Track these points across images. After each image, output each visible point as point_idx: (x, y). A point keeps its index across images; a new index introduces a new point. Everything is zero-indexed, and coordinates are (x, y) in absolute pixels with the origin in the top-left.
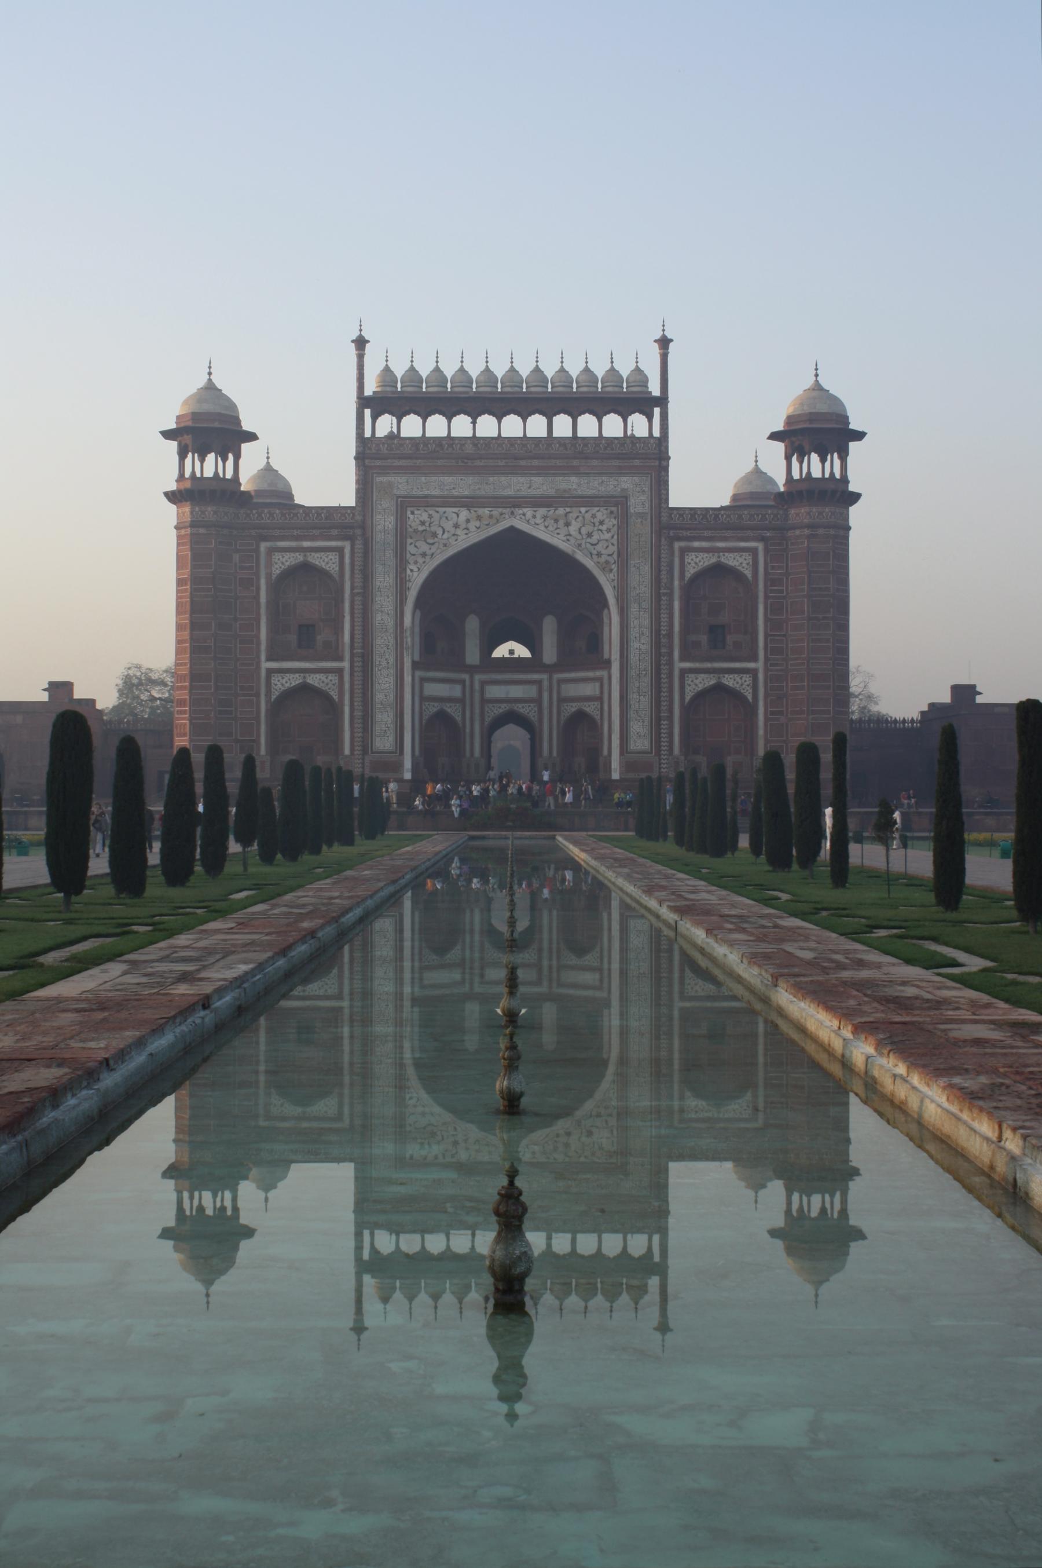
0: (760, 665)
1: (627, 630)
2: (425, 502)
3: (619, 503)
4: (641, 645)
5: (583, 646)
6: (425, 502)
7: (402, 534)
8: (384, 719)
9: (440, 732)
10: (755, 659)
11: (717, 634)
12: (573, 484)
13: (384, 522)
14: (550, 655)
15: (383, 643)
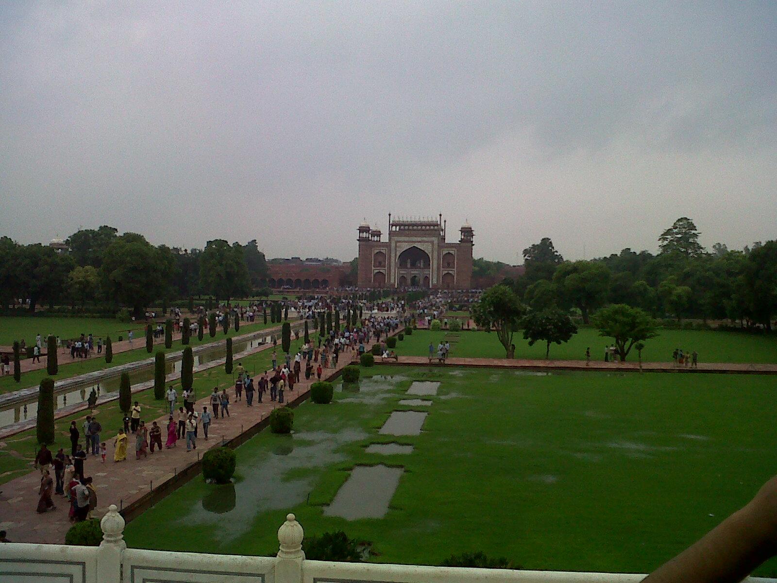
0: (455, 269)
1: (434, 263)
2: (400, 242)
3: (432, 242)
4: (435, 266)
5: (427, 265)
6: (400, 242)
7: (396, 246)
8: (392, 278)
9: (403, 279)
10: (454, 268)
11: (449, 264)
12: (425, 239)
13: (393, 245)
14: (422, 266)
15: (393, 264)
